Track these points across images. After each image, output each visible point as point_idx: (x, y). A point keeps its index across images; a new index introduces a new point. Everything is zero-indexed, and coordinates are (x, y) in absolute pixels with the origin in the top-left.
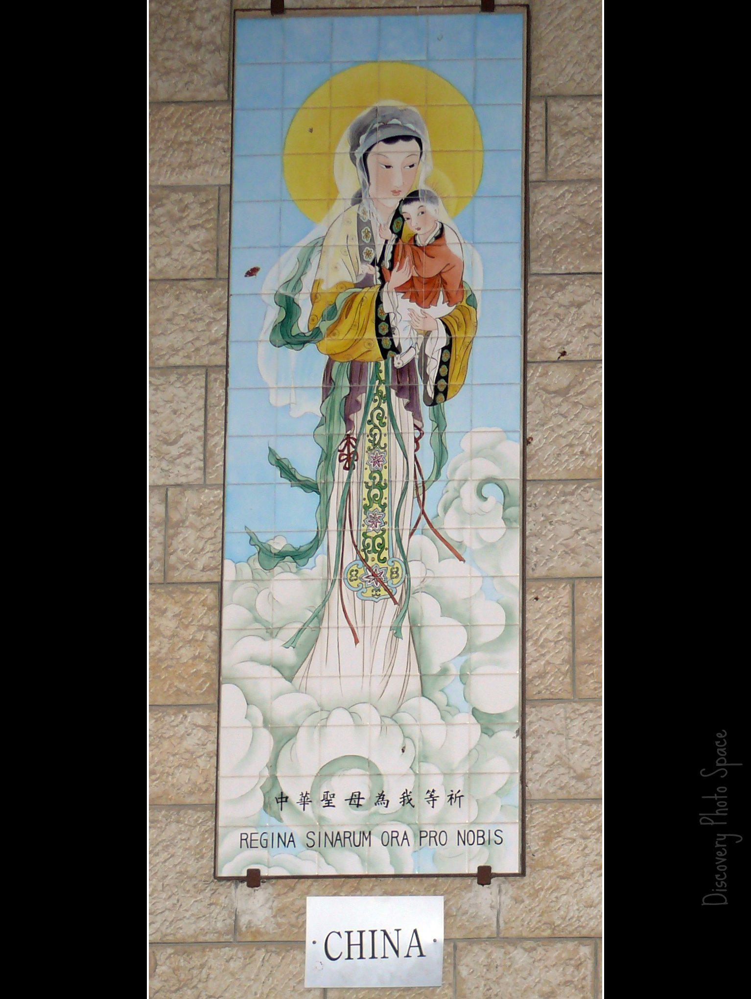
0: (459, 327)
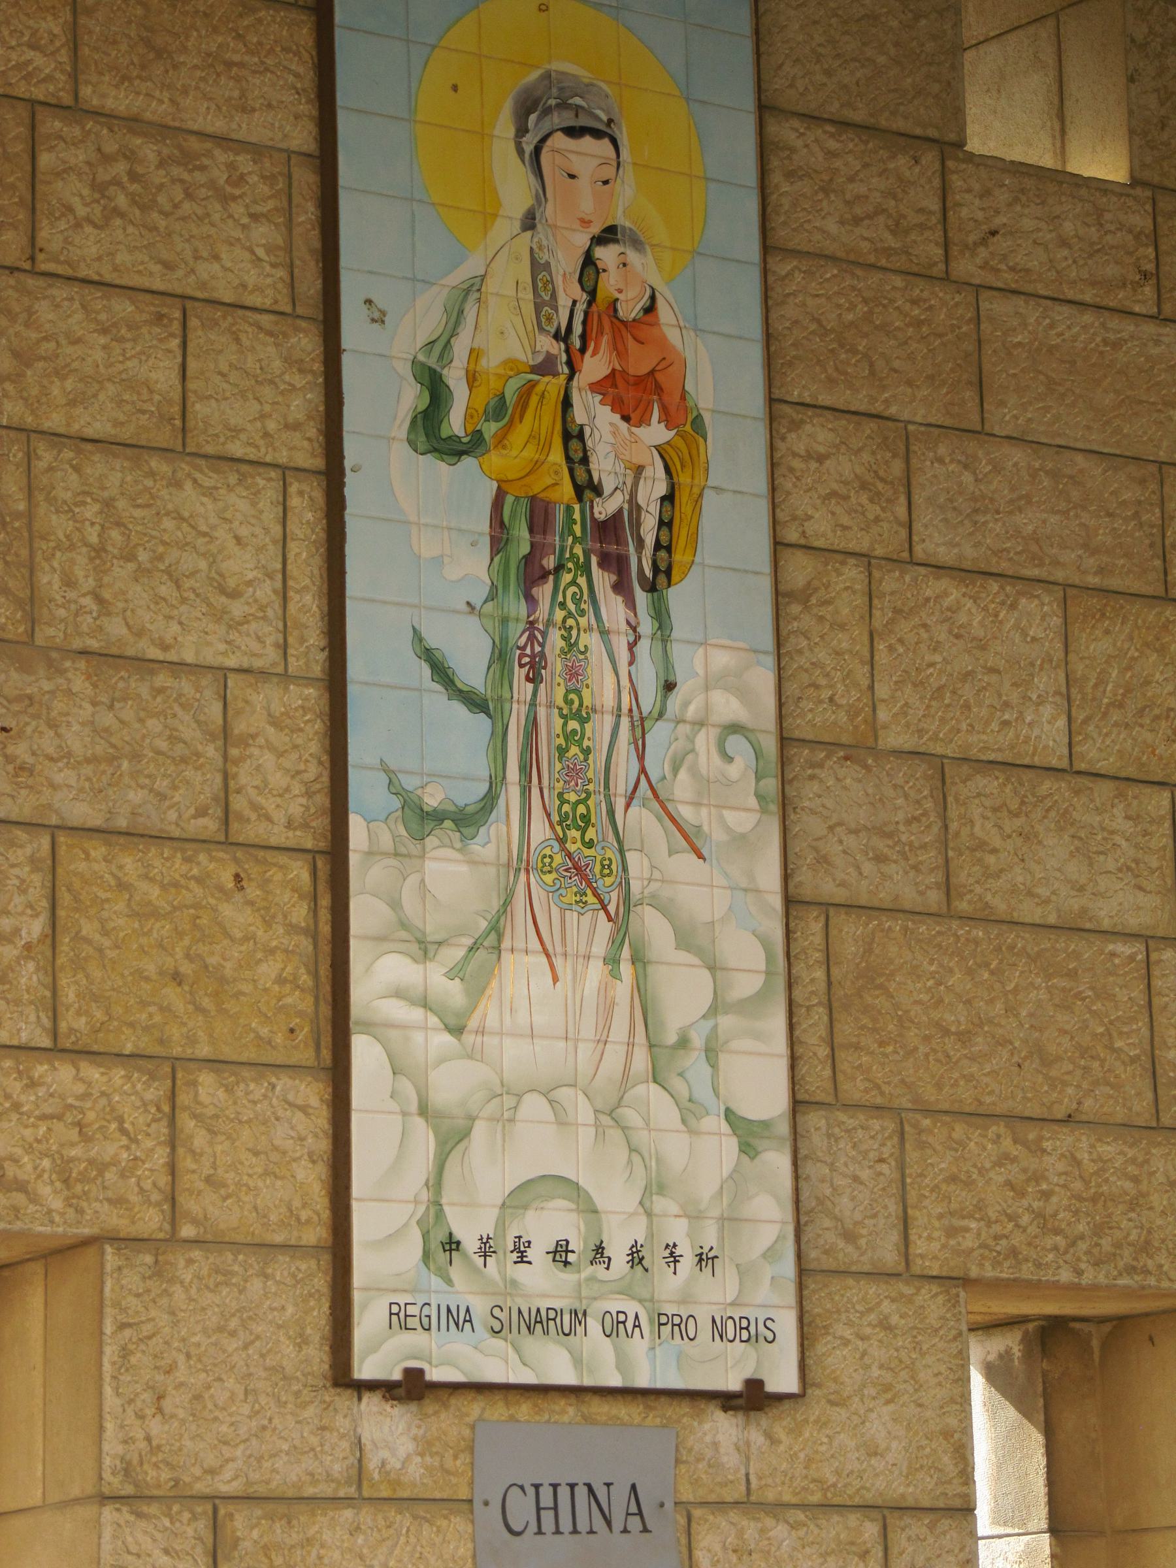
0: (683, 466)
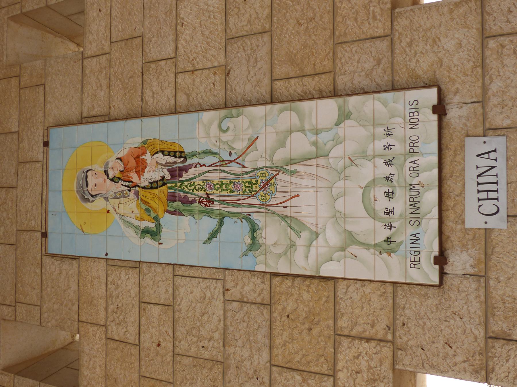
0: (155, 148)
